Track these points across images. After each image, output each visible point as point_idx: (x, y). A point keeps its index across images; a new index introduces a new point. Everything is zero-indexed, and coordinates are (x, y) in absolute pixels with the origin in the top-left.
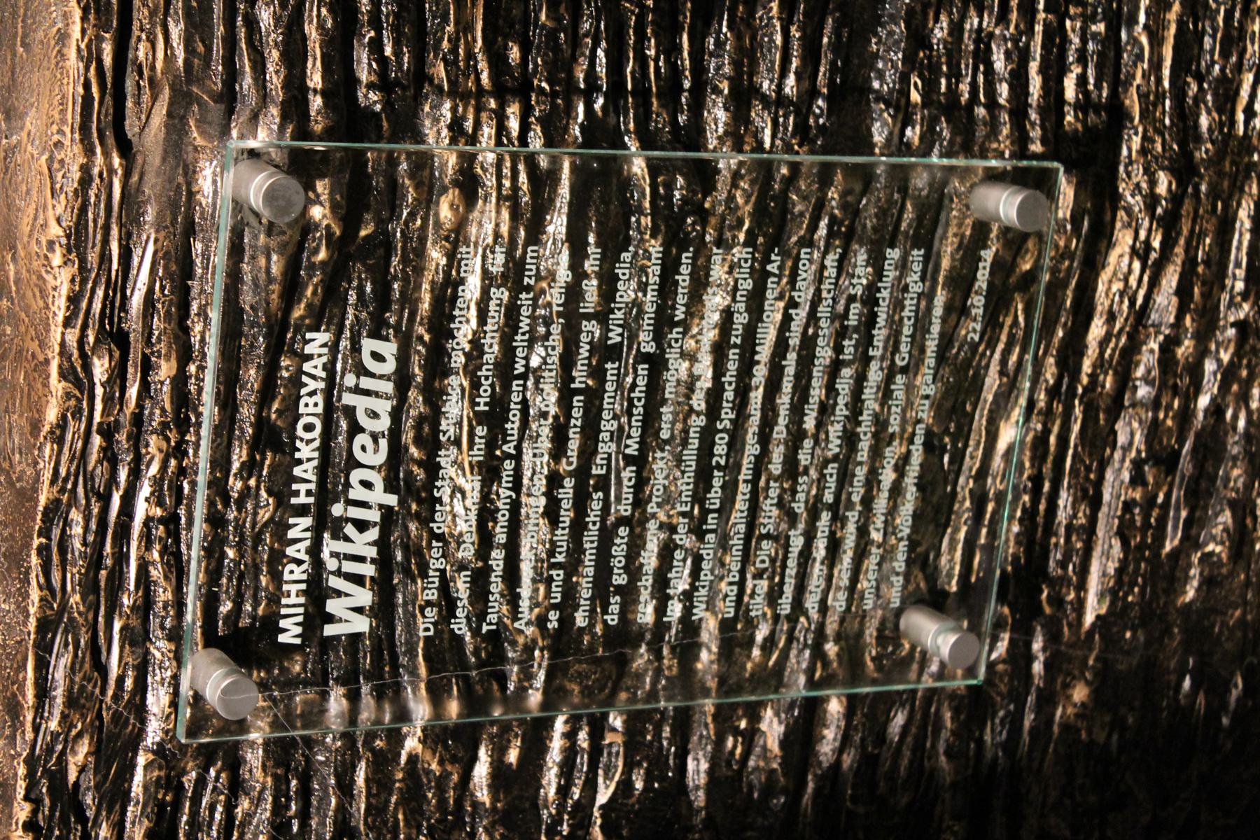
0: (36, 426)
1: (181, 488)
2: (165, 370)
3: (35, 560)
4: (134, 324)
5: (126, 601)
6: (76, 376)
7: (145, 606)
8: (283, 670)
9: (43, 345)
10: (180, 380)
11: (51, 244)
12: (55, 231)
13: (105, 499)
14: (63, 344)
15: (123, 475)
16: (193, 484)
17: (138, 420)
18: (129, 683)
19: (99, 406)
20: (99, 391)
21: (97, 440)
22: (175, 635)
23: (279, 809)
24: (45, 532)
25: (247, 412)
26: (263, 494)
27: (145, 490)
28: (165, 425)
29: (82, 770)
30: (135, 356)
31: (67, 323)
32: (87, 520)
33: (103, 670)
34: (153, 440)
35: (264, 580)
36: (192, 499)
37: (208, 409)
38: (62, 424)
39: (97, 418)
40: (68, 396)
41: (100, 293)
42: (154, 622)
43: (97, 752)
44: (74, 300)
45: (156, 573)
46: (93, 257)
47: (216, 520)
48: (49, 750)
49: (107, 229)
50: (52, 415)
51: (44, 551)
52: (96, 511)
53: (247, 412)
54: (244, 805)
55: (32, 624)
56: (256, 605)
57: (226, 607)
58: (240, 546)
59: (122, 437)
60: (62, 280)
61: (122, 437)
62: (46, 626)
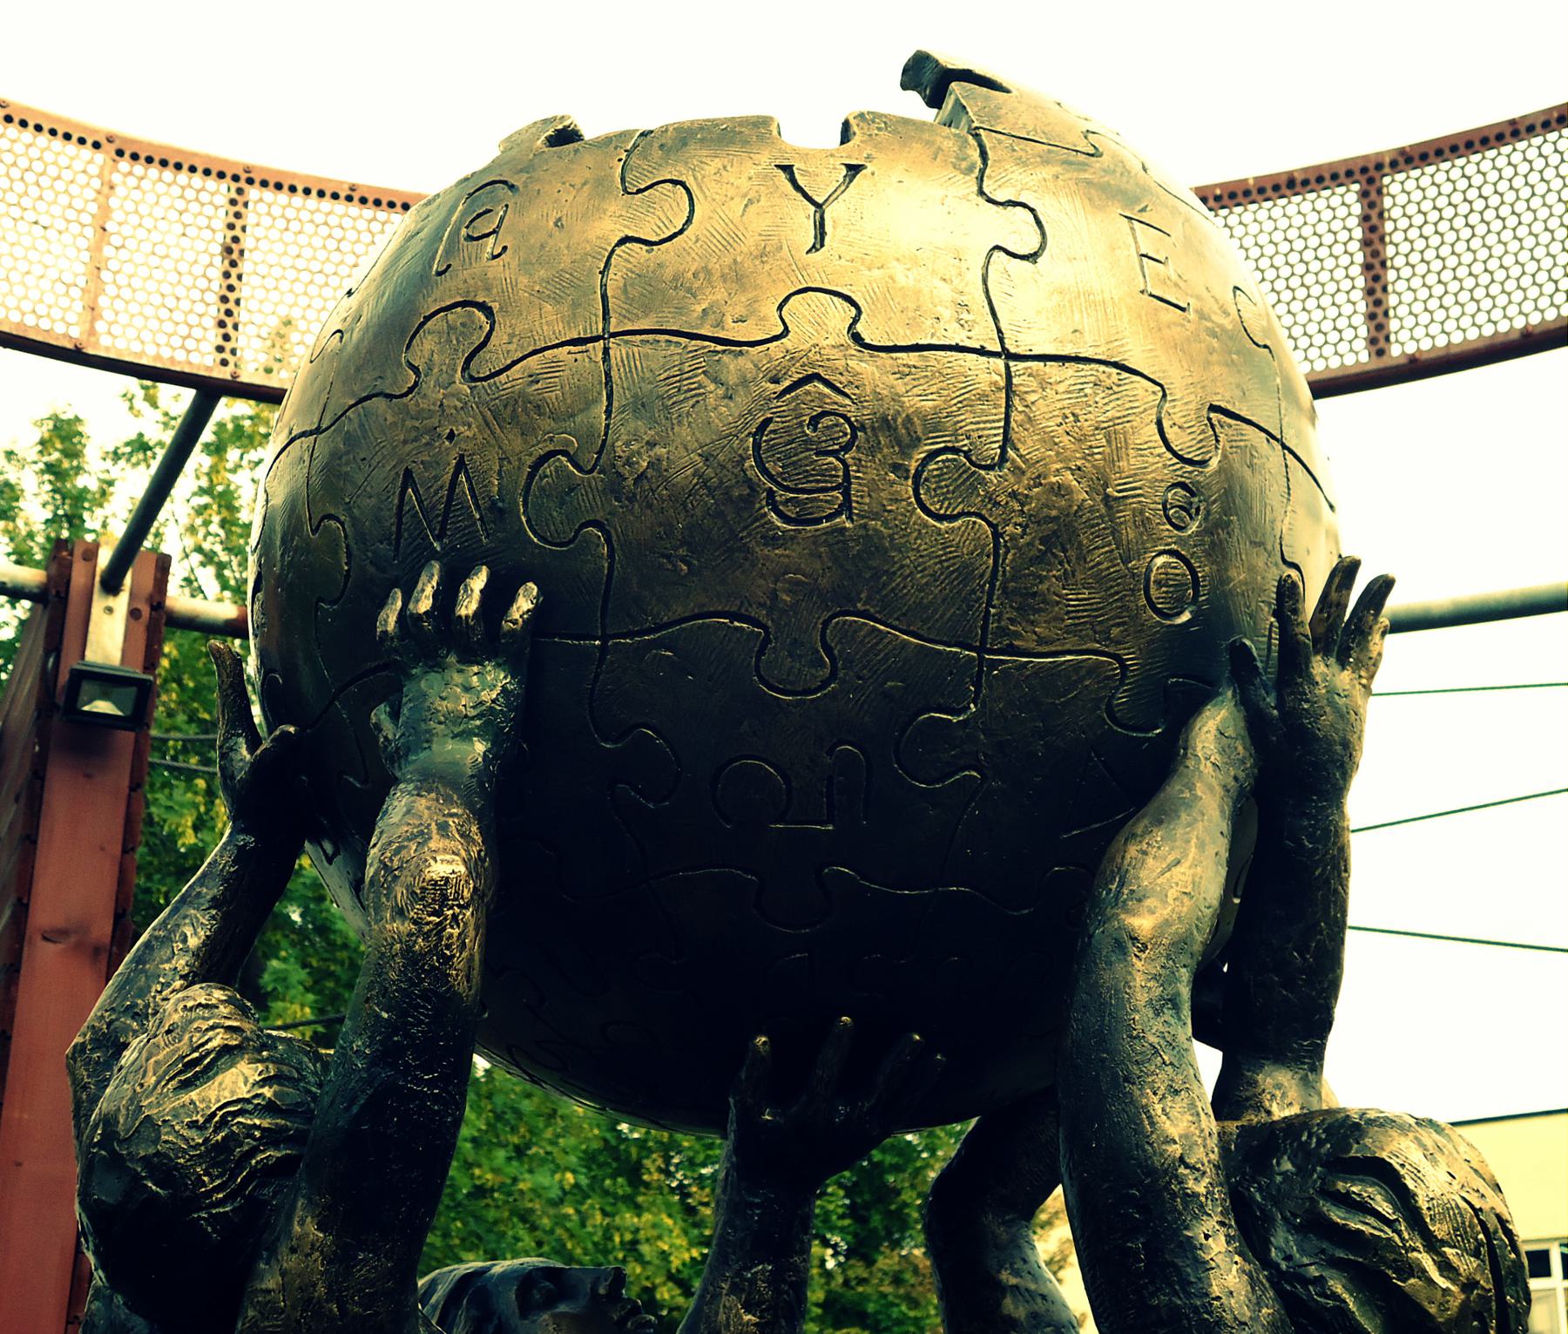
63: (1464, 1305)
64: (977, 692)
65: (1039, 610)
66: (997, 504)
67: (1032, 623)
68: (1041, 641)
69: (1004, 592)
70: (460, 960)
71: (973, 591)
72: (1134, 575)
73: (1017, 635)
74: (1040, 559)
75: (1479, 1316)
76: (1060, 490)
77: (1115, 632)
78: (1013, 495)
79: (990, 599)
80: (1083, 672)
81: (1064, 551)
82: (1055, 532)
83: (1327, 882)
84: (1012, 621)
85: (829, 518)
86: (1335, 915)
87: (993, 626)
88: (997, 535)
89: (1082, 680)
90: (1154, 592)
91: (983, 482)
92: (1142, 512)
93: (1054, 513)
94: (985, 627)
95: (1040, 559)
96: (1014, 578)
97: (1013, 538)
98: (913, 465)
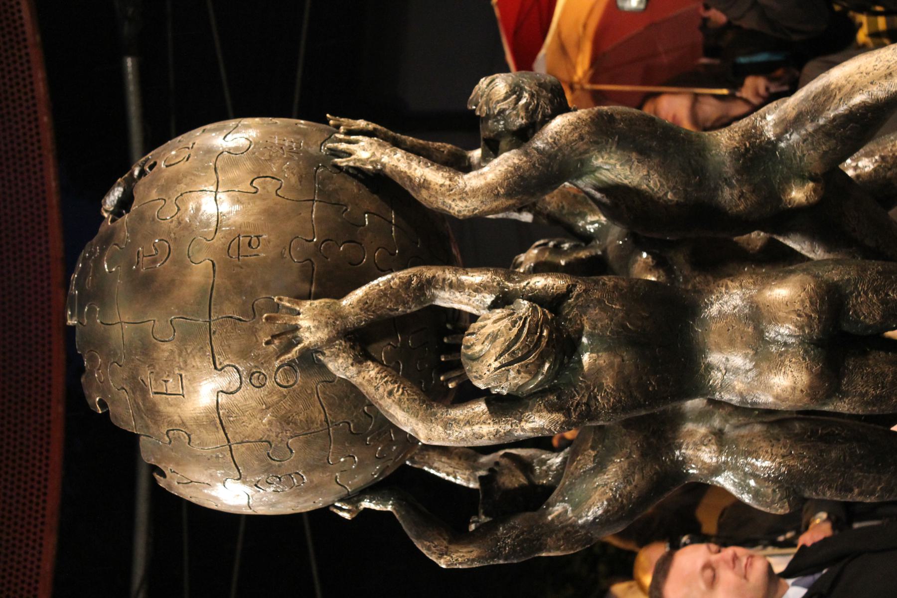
63: (525, 372)
64: (341, 423)
65: (311, 417)
66: (282, 440)
67: (315, 418)
68: (320, 412)
69: (308, 430)
70: (468, 556)
71: (312, 438)
72: (289, 392)
73: (321, 421)
74: (295, 423)
75: (527, 367)
76: (270, 423)
77: (309, 392)
78: (277, 436)
79: (314, 432)
80: (325, 396)
81: (289, 417)
82: (285, 422)
83: (373, 312)
84: (317, 424)
85: (300, 475)
86: (383, 302)
87: (321, 429)
88: (292, 437)
89: (327, 395)
90: (291, 383)
91: (276, 445)
92: (267, 395)
93: (278, 424)
94: (322, 431)
95: (295, 423)
96: (303, 428)
97: (291, 433)
98: (277, 463)
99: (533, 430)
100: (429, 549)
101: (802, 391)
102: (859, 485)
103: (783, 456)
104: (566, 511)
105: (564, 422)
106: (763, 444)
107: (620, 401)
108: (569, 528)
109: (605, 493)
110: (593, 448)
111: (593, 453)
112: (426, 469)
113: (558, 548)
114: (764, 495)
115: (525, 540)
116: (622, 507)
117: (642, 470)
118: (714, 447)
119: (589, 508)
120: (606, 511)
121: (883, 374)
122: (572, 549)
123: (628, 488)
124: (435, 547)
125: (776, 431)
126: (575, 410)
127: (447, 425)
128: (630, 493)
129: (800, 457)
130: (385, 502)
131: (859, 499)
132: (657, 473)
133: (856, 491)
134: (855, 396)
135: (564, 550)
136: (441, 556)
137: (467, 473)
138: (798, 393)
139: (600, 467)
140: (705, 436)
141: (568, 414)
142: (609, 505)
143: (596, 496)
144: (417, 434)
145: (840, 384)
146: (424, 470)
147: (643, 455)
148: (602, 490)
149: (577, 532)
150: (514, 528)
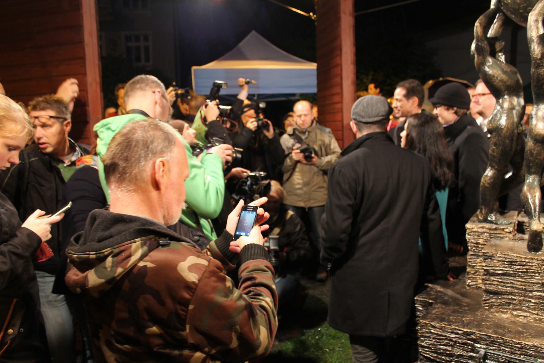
0: (512, 338)
1: (504, 351)
2: (518, 352)
3: (497, 336)
4: (524, 350)
5: (491, 344)
6: (518, 343)
7: (490, 346)
8: (481, 359)
9: (522, 340)
10: (517, 354)
11: (534, 343)
12: (536, 344)
13: (503, 344)
14: (522, 343)
15: (506, 346)
16: (504, 353)
17: (513, 349)
18: (482, 343)
19: (514, 345)
20: (516, 346)
21: (511, 344)
22: (487, 349)
23: (465, 356)
24: (500, 338)
25: (512, 360)
26: (503, 360)
27: (504, 348)
28: (512, 351)
29: (472, 337)
30: (520, 350)
31: (525, 344)
32: (502, 342)
33: (484, 341)
34: (510, 350)
35: (492, 359)
36: (502, 353)
37: (513, 357)
38: (513, 341)
39: (513, 345)
40: (516, 342)
41: (528, 347)
42: (489, 346)
43: (474, 339)
44: (527, 345)
45: (494, 348)
46: (532, 347)
47: (500, 355)
48: (475, 334)
49: (536, 349)
50: (514, 340)
51: (498, 337)
52: (502, 343)
53: (512, 360)
54: (466, 352)
55: (490, 335)
56: (490, 357)
57: (489, 354)
58: (496, 357)
59: (510, 347)
60: (530, 343)
61: (510, 347)
62: (490, 336)
99: (534, 49)
100: (481, 20)
101: (539, 132)
102: (497, 148)
103: (508, 127)
104: (489, 62)
105: (537, 58)
106: (511, 121)
107: (542, 76)
108: (484, 64)
109: (496, 74)
110: (510, 71)
111: (509, 70)
112: (496, 20)
113: (478, 60)
114: (494, 121)
115: (482, 50)
116: (491, 79)
117: (503, 85)
118: (510, 107)
119: (491, 69)
120: (490, 75)
121: (540, 156)
122: (477, 64)
123: (497, 81)
124: (483, 22)
125: (515, 125)
126: (541, 62)
127: (537, 21)
128: (496, 82)
129: (507, 132)
130: (494, 5)
131: (491, 148)
132: (501, 90)
133: (495, 148)
134: (534, 147)
135: (477, 62)
136: (480, 24)
137: (494, 34)
138: (538, 130)
139: (505, 72)
140: (513, 104)
141: (540, 59)
142: (492, 76)
143: (495, 71)
144: (534, 11)
145: (539, 143)
146: (494, 20)
147: (508, 86)
148: (497, 74)
149: (483, 66)
150: (487, 46)
